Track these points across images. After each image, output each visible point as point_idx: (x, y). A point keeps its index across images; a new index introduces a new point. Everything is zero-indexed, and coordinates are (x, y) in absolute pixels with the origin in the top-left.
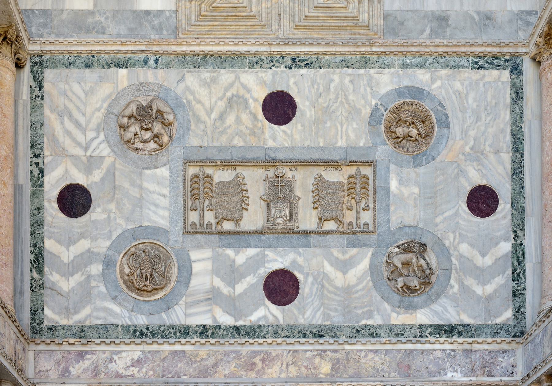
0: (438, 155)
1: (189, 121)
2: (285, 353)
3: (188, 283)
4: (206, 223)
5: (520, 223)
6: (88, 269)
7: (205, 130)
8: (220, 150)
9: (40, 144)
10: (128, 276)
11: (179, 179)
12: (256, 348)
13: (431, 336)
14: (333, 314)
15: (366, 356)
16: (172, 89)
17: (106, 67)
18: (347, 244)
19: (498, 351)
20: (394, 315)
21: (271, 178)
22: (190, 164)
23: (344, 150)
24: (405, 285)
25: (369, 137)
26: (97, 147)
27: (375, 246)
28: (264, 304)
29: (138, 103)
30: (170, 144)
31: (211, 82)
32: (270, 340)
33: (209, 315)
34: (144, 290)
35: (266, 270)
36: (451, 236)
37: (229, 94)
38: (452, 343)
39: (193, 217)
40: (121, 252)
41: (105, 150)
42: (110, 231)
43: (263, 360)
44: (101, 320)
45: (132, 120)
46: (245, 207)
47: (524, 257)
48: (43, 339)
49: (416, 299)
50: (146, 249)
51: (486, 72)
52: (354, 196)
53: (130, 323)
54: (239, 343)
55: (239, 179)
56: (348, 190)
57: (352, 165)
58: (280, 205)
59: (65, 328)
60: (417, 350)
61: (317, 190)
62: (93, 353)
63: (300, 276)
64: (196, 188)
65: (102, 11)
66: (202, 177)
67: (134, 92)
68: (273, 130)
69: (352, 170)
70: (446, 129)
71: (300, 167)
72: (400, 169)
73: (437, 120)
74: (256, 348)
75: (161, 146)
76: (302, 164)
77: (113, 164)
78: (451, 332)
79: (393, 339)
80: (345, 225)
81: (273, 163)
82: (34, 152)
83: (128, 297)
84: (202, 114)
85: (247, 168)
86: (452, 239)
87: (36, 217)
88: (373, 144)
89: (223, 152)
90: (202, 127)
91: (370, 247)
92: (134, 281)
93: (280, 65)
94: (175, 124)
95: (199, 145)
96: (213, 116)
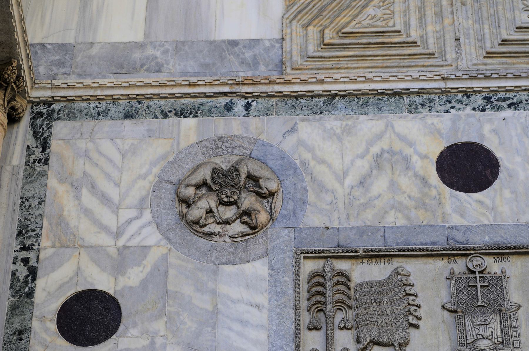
1: (305, 189)
7: (334, 202)
8: (362, 232)
9: (33, 230)
16: (275, 144)
17: (160, 116)
21: (460, 274)
22: (306, 255)
29: (214, 166)
30: (270, 224)
31: (342, 133)
37: (375, 149)
45: (203, 191)
46: (415, 322)
55: (399, 277)
58: (482, 318)
64: (318, 293)
65: (158, 43)
66: (329, 275)
67: (207, 151)
68: (459, 200)
71: (514, 256)
75: (253, 228)
77: (165, 258)
82: (23, 242)
84: (330, 181)
85: (413, 260)
89: (368, 235)
90: (328, 198)
93: (464, 106)
94: (280, 195)
95: (323, 226)
96: (349, 181)
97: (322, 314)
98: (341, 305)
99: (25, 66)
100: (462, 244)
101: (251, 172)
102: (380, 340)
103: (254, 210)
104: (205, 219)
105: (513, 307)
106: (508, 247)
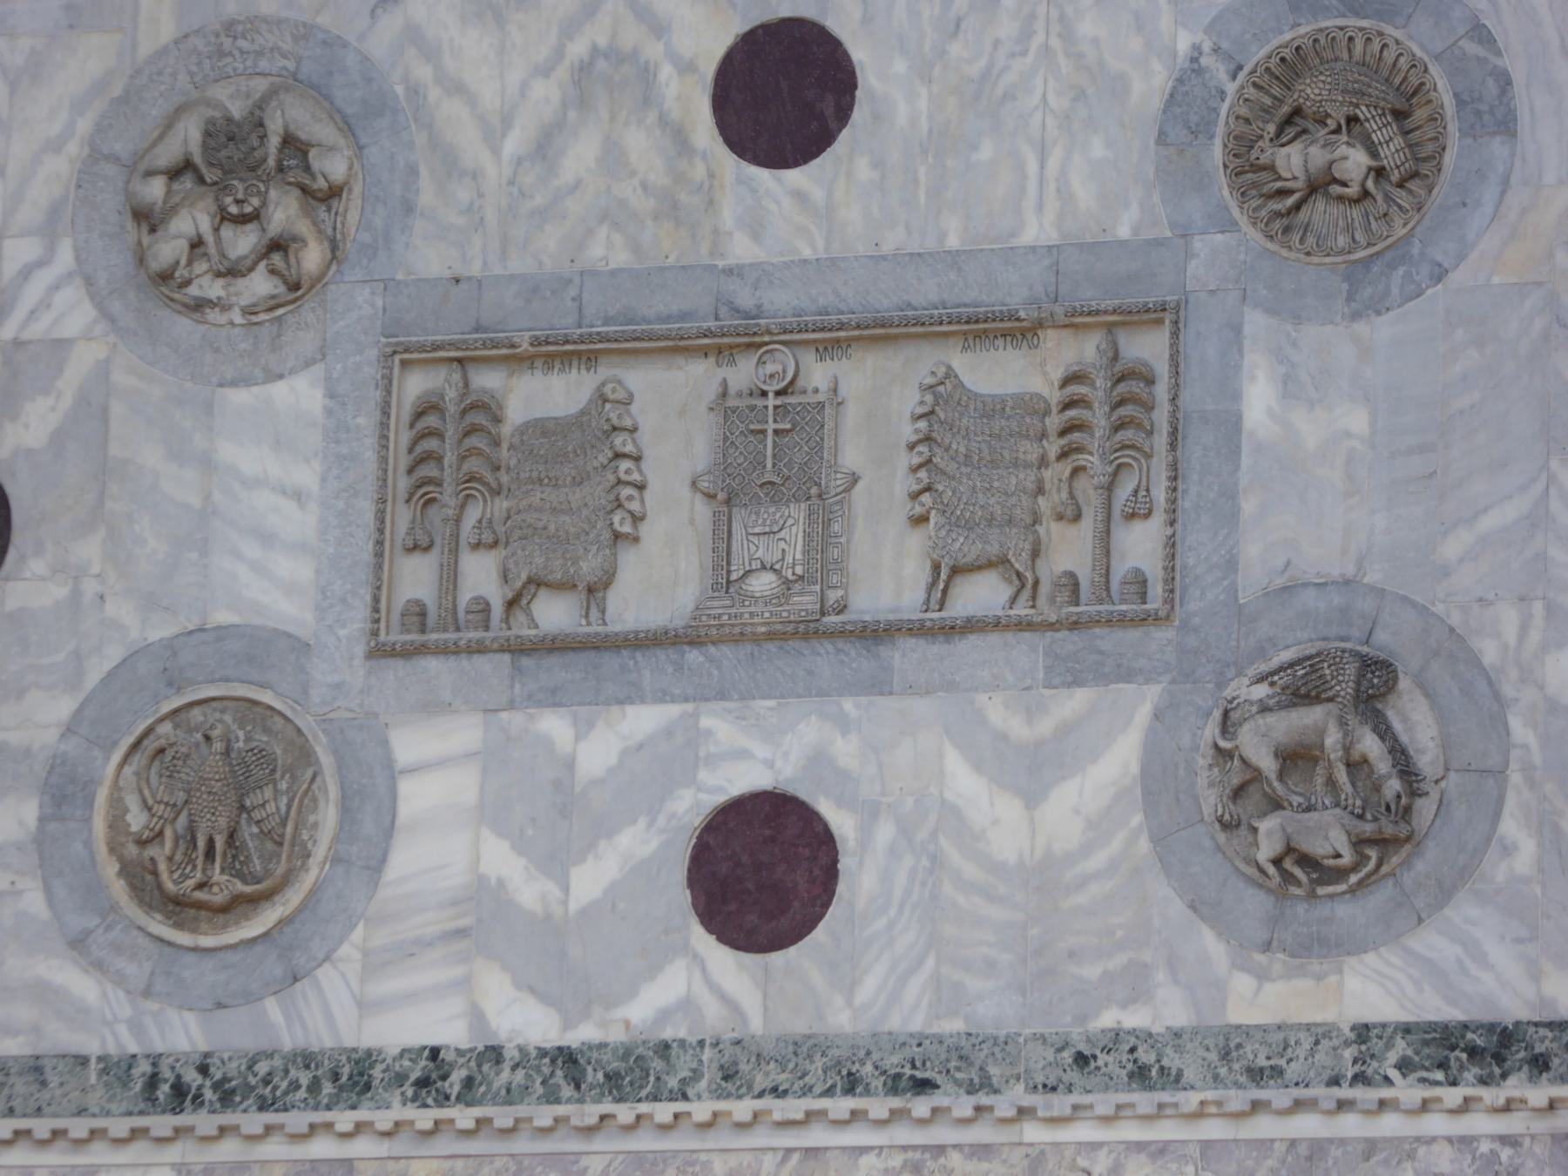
0: (1461, 257)
1: (413, 171)
2: (769, 1161)
3: (377, 866)
4: (465, 598)
11: (361, 420)
13: (1404, 1076)
14: (974, 984)
18: (1049, 669)
20: (1243, 983)
21: (740, 394)
22: (406, 356)
23: (1046, 262)
24: (1289, 850)
25: (1156, 198)
26: (45, 304)
27: (1167, 678)
28: (686, 949)
29: (210, 113)
30: (331, 273)
32: (701, 1110)
33: (457, 1005)
34: (199, 905)
35: (702, 796)
36: (1509, 618)
37: (578, 49)
40: (115, 744)
42: (78, 656)
44: (21, 1039)
45: (187, 182)
46: (627, 528)
50: (212, 727)
53: (133, 1048)
56: (1063, 433)
57: (1085, 326)
60: (1342, 1142)
61: (928, 439)
67: (199, 64)
68: (754, 191)
70: (1498, 139)
72: (1289, 327)
73: (1460, 103)
75: (294, 286)
76: (866, 332)
77: (103, 370)
78: (1499, 1059)
79: (1232, 1092)
83: (135, 932)
86: (1511, 633)
88: (1173, 225)
90: (463, 194)
91: (1147, 682)
92: (162, 867)
94: (357, 189)
95: (447, 274)
96: (512, 145)
100: (747, 316)
101: (292, 128)
102: (549, 577)
104: (190, 263)
105: (839, 482)
106: (843, 324)
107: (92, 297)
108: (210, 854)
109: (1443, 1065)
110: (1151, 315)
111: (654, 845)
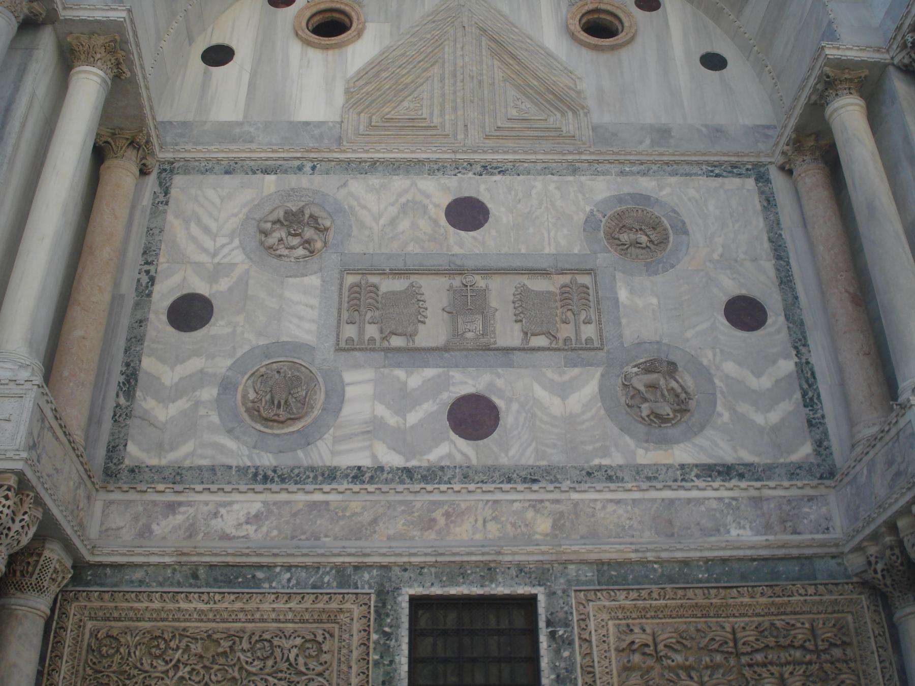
1: (351, 227)
2: (481, 505)
3: (338, 411)
5: (801, 337)
6: (197, 393)
9: (155, 251)
10: (253, 402)
12: (437, 497)
13: (698, 479)
14: (549, 451)
15: (604, 507)
17: (250, 173)
19: (801, 498)
20: (640, 452)
24: (652, 413)
36: (710, 354)
37: (403, 200)
38: (732, 489)
39: (350, 331)
40: (246, 373)
41: (238, 257)
43: (447, 515)
45: (278, 226)
47: (814, 378)
48: (120, 485)
49: (670, 431)
51: (726, 180)
52: (570, 307)
53: (249, 464)
54: (411, 490)
57: (566, 273)
59: (153, 471)
60: (679, 499)
62: (189, 504)
63: (499, 403)
69: (566, 279)
73: (672, 227)
74: (437, 497)
75: (312, 252)
77: (247, 272)
79: (642, 483)
80: (561, 341)
81: (461, 271)
82: (146, 259)
85: (424, 277)
87: (135, 331)
90: (367, 233)
91: (598, 366)
92: (262, 409)
94: (333, 229)
96: (382, 222)
97: (357, 312)
98: (371, 307)
99: (153, 133)
101: (313, 213)
103: (313, 240)
107: (244, 253)
108: (279, 406)
109: (710, 476)
110: (588, 272)
111: (435, 408)
